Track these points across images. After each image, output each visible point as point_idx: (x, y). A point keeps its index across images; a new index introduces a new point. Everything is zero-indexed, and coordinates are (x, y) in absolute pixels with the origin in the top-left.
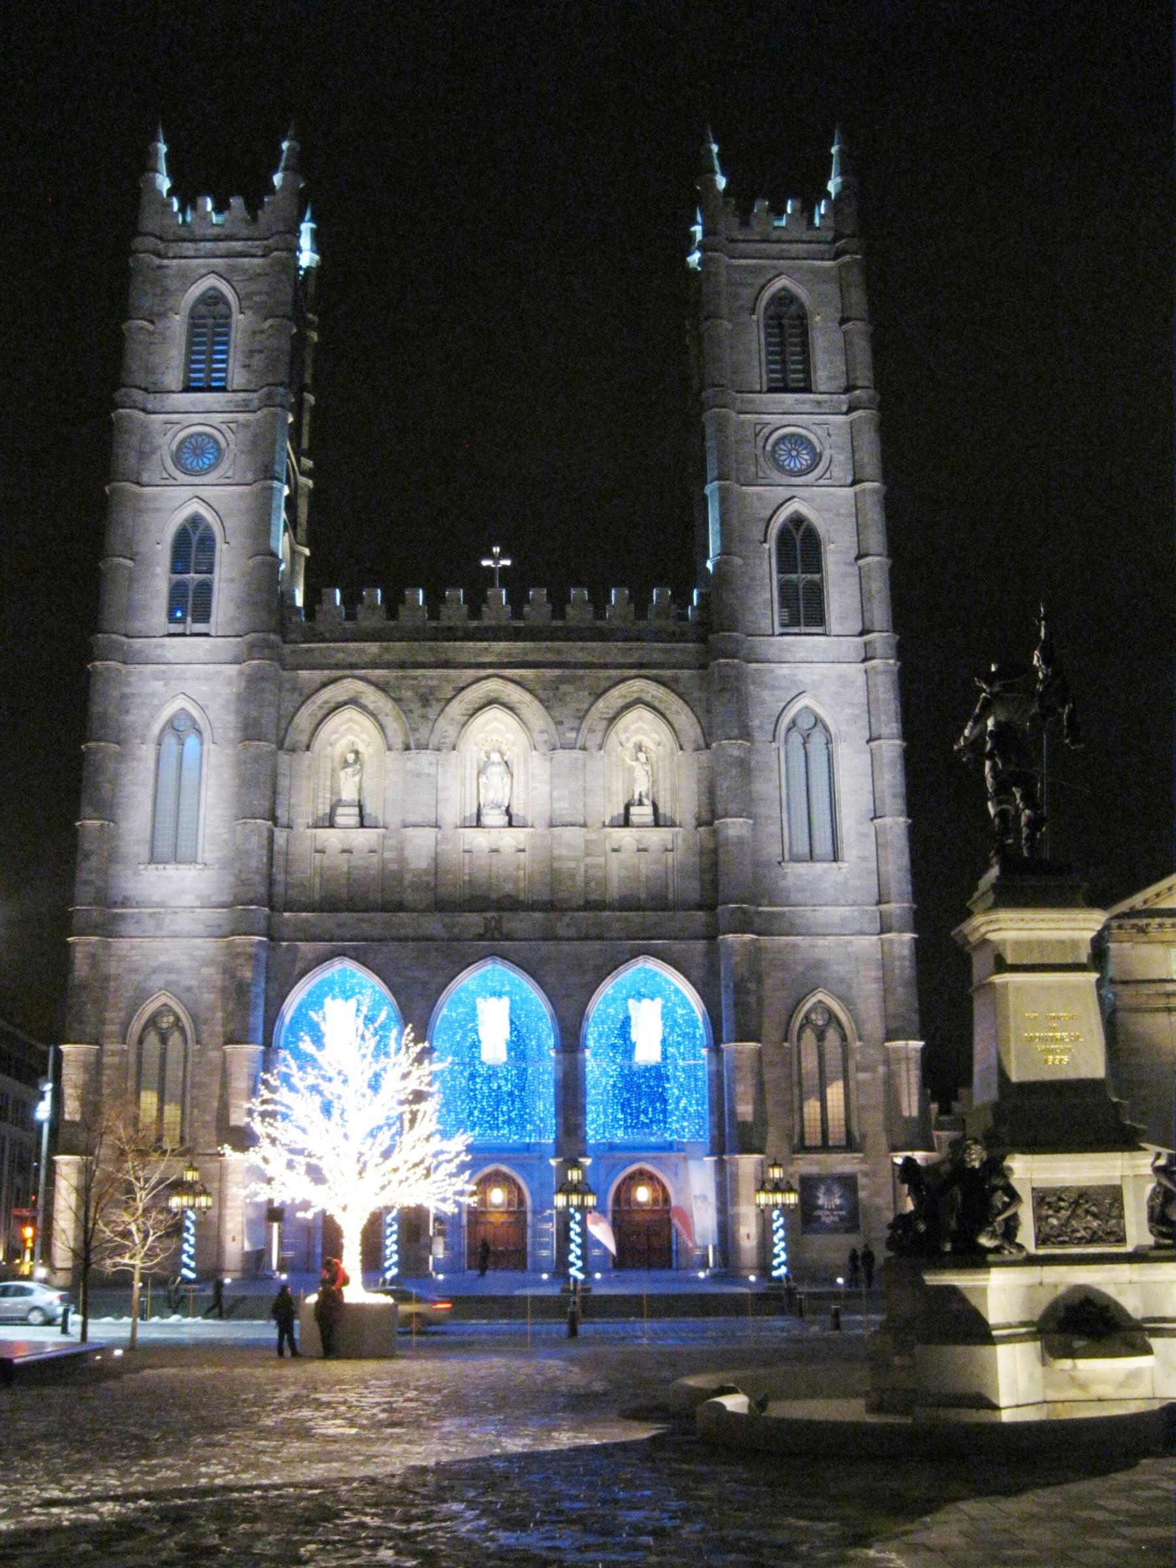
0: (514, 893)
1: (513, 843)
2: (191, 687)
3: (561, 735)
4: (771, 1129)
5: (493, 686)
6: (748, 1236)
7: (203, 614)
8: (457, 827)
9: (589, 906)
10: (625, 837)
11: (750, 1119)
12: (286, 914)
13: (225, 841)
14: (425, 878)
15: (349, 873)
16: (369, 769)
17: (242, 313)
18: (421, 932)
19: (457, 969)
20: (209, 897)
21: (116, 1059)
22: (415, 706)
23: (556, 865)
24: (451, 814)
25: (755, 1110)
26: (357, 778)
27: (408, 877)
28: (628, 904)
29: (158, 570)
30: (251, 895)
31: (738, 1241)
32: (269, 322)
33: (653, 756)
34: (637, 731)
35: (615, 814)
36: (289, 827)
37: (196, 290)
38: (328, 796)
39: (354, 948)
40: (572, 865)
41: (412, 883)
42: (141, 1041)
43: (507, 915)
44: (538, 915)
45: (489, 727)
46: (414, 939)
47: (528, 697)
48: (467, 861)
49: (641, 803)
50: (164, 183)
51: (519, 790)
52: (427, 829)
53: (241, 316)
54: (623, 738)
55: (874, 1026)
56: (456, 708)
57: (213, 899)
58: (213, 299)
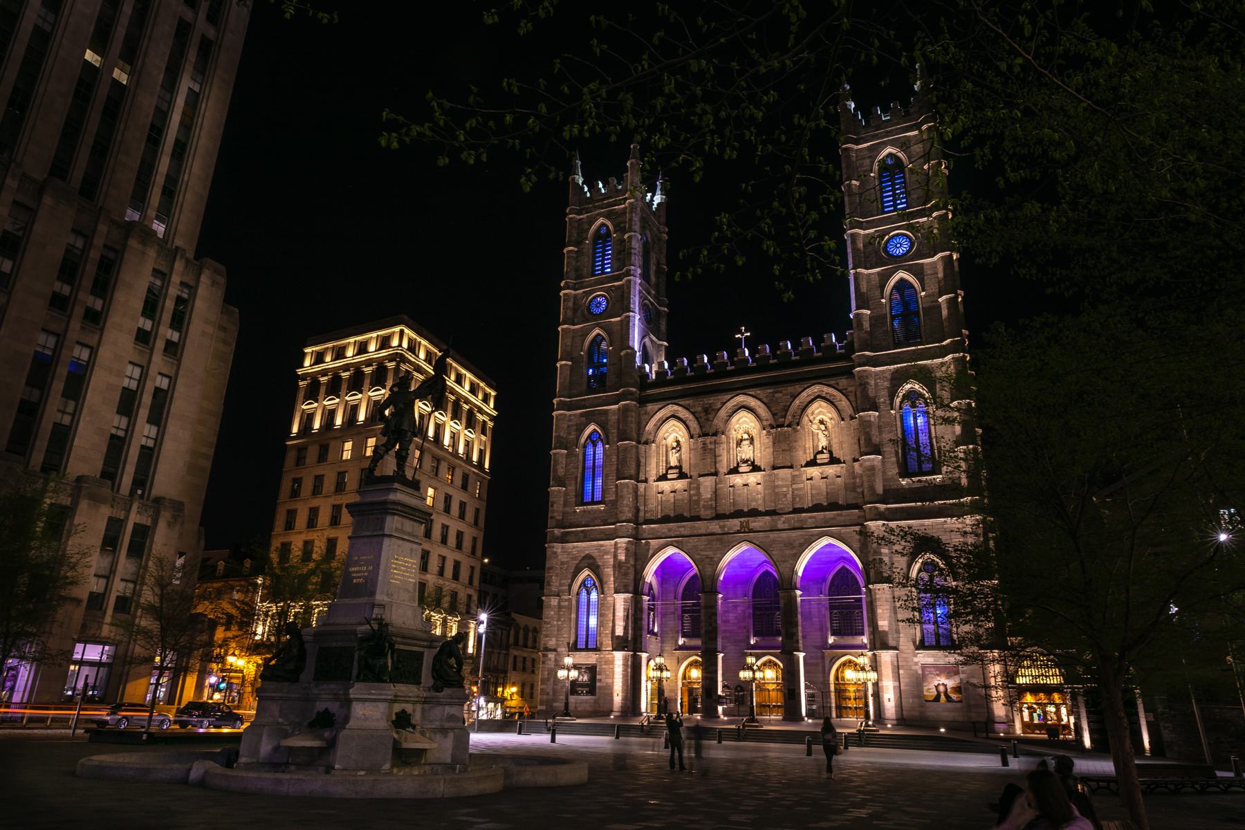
3: (775, 420)
4: (901, 635)
5: (741, 399)
9: (796, 511)
10: (814, 472)
11: (886, 629)
12: (644, 526)
16: (685, 448)
18: (709, 531)
19: (727, 549)
20: (606, 520)
21: (567, 603)
22: (702, 415)
25: (890, 624)
27: (702, 503)
28: (817, 508)
33: (829, 425)
34: (819, 413)
35: (809, 460)
39: (675, 541)
40: (785, 489)
42: (578, 594)
43: (751, 519)
44: (767, 518)
45: (741, 421)
46: (705, 535)
47: (759, 403)
48: (732, 492)
49: (821, 452)
52: (710, 478)
54: (811, 418)
56: (723, 413)
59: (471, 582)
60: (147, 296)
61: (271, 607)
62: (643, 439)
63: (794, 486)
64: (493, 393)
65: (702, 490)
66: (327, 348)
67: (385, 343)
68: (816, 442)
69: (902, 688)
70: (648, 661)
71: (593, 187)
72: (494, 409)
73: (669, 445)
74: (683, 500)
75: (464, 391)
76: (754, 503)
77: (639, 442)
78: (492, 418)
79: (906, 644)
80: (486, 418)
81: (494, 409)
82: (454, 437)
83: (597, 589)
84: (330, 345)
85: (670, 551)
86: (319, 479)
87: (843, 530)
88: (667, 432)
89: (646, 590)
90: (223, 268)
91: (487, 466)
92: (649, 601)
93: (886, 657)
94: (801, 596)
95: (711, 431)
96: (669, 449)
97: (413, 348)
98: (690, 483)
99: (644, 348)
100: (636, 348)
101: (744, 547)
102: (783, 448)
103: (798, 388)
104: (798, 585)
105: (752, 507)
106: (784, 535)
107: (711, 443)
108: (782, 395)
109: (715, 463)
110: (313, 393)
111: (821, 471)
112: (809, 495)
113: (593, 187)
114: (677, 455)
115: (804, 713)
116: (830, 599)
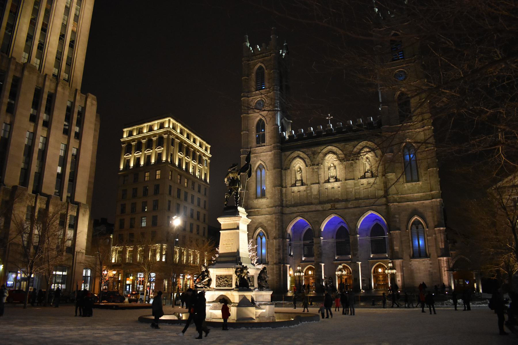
0: (338, 198)
1: (337, 185)
2: (262, 158)
4: (404, 253)
6: (399, 281)
7: (264, 141)
8: (323, 183)
9: (356, 199)
10: (364, 181)
11: (398, 250)
13: (271, 192)
14: (316, 196)
15: (300, 197)
16: (303, 172)
17: (266, 70)
18: (317, 209)
23: (347, 190)
24: (322, 181)
26: (300, 174)
29: (253, 133)
30: (277, 204)
31: (396, 282)
32: (272, 71)
33: (371, 159)
35: (362, 175)
36: (286, 187)
37: (256, 67)
38: (294, 179)
39: (301, 214)
40: (351, 189)
41: (314, 198)
42: (256, 239)
46: (315, 211)
49: (368, 172)
50: (248, 45)
51: (338, 172)
52: (316, 185)
53: (266, 71)
55: (431, 224)
56: (321, 155)
57: (270, 206)
58: (260, 68)
59: (204, 235)
60: (66, 113)
61: (118, 248)
62: (284, 167)
63: (356, 188)
64: (209, 146)
65: (312, 190)
66: (134, 129)
67: (162, 126)
68: (365, 167)
69: (404, 275)
70: (290, 268)
71: (254, 48)
72: (210, 154)
73: (296, 170)
74: (304, 195)
75: (197, 146)
76: (337, 196)
77: (282, 169)
78: (210, 158)
79: (406, 256)
80: (207, 158)
81: (210, 154)
82: (194, 168)
83: (265, 236)
84: (135, 127)
85: (299, 219)
86: (135, 190)
87: (378, 207)
88: (295, 164)
89: (288, 237)
90: (95, 97)
91: (208, 181)
92: (289, 241)
93: (398, 262)
94: (359, 237)
95: (316, 163)
96: (296, 172)
97: (174, 128)
98: (307, 187)
99: (282, 124)
100: (279, 125)
101: (333, 216)
102: (350, 170)
103: (356, 143)
104: (358, 233)
105: (336, 198)
106: (351, 210)
107: (316, 169)
108: (349, 146)
109: (318, 178)
110: (129, 150)
111: (367, 180)
112: (362, 192)
113: (254, 48)
114: (300, 174)
115: (361, 288)
116: (371, 238)
